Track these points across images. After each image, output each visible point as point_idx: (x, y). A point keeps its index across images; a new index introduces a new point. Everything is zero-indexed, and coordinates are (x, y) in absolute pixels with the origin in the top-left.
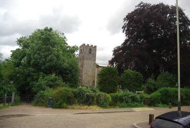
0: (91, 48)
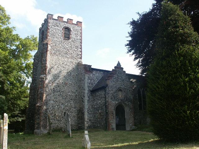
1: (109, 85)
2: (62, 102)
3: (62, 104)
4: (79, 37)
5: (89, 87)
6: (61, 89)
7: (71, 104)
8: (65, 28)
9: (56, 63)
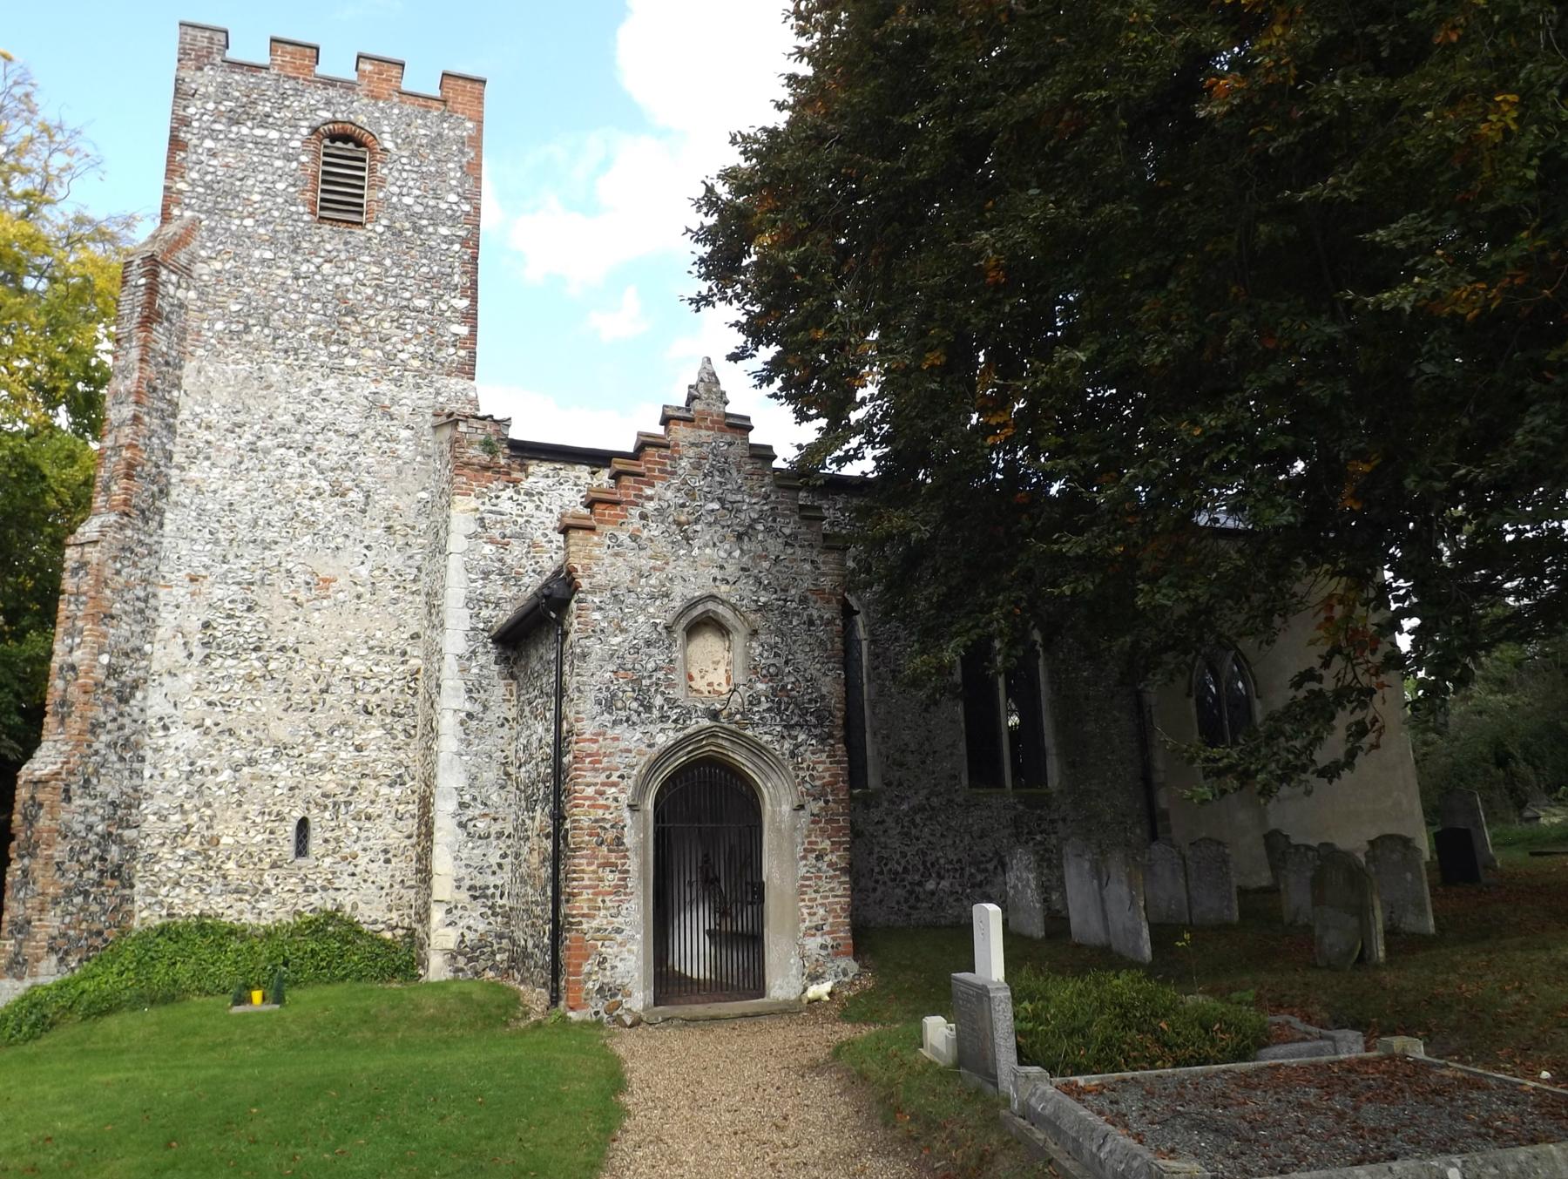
0: (361, 114)
1: (584, 584)
2: (281, 732)
3: (280, 750)
4: (453, 198)
5: (475, 602)
6: (277, 624)
7: (359, 749)
8: (334, 138)
9: (239, 419)
